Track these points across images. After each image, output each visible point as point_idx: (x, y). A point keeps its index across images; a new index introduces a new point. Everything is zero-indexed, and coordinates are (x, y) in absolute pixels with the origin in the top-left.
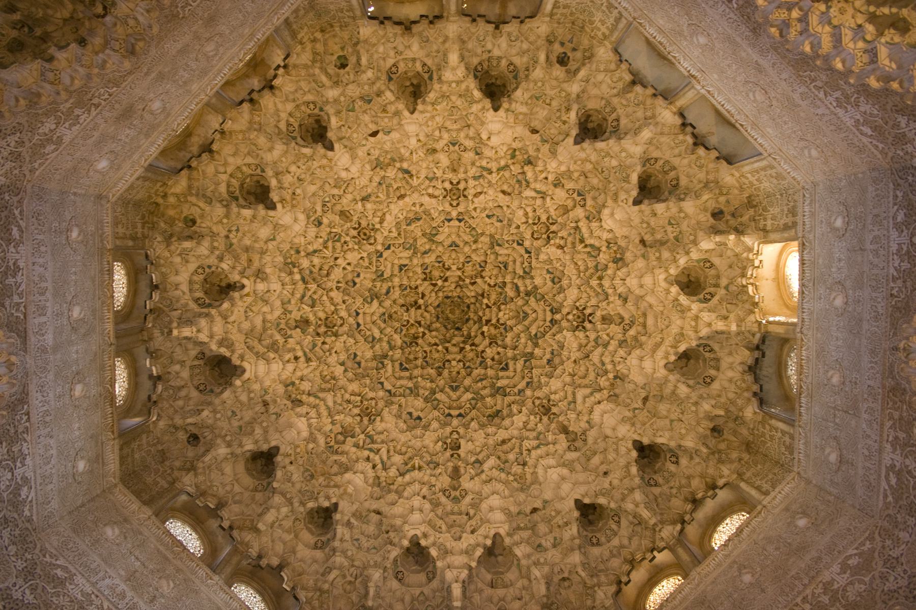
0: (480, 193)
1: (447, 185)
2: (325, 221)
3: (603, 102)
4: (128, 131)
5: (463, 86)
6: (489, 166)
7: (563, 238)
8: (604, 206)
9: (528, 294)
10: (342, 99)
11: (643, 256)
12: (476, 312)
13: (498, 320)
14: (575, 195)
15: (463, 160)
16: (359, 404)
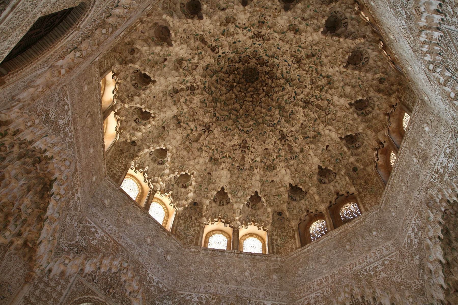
0: (275, 143)
1: (289, 138)
2: (326, 102)
3: (257, 207)
4: (422, 146)
5: (307, 187)
6: (279, 158)
7: (236, 149)
8: (231, 176)
9: (230, 113)
10: (347, 157)
11: (205, 170)
12: (242, 83)
13: (233, 90)
14: (242, 167)
15: (289, 153)
16: (264, 37)
